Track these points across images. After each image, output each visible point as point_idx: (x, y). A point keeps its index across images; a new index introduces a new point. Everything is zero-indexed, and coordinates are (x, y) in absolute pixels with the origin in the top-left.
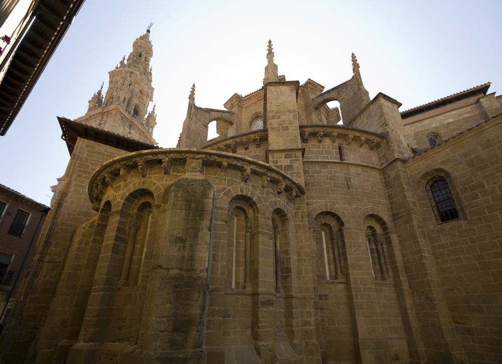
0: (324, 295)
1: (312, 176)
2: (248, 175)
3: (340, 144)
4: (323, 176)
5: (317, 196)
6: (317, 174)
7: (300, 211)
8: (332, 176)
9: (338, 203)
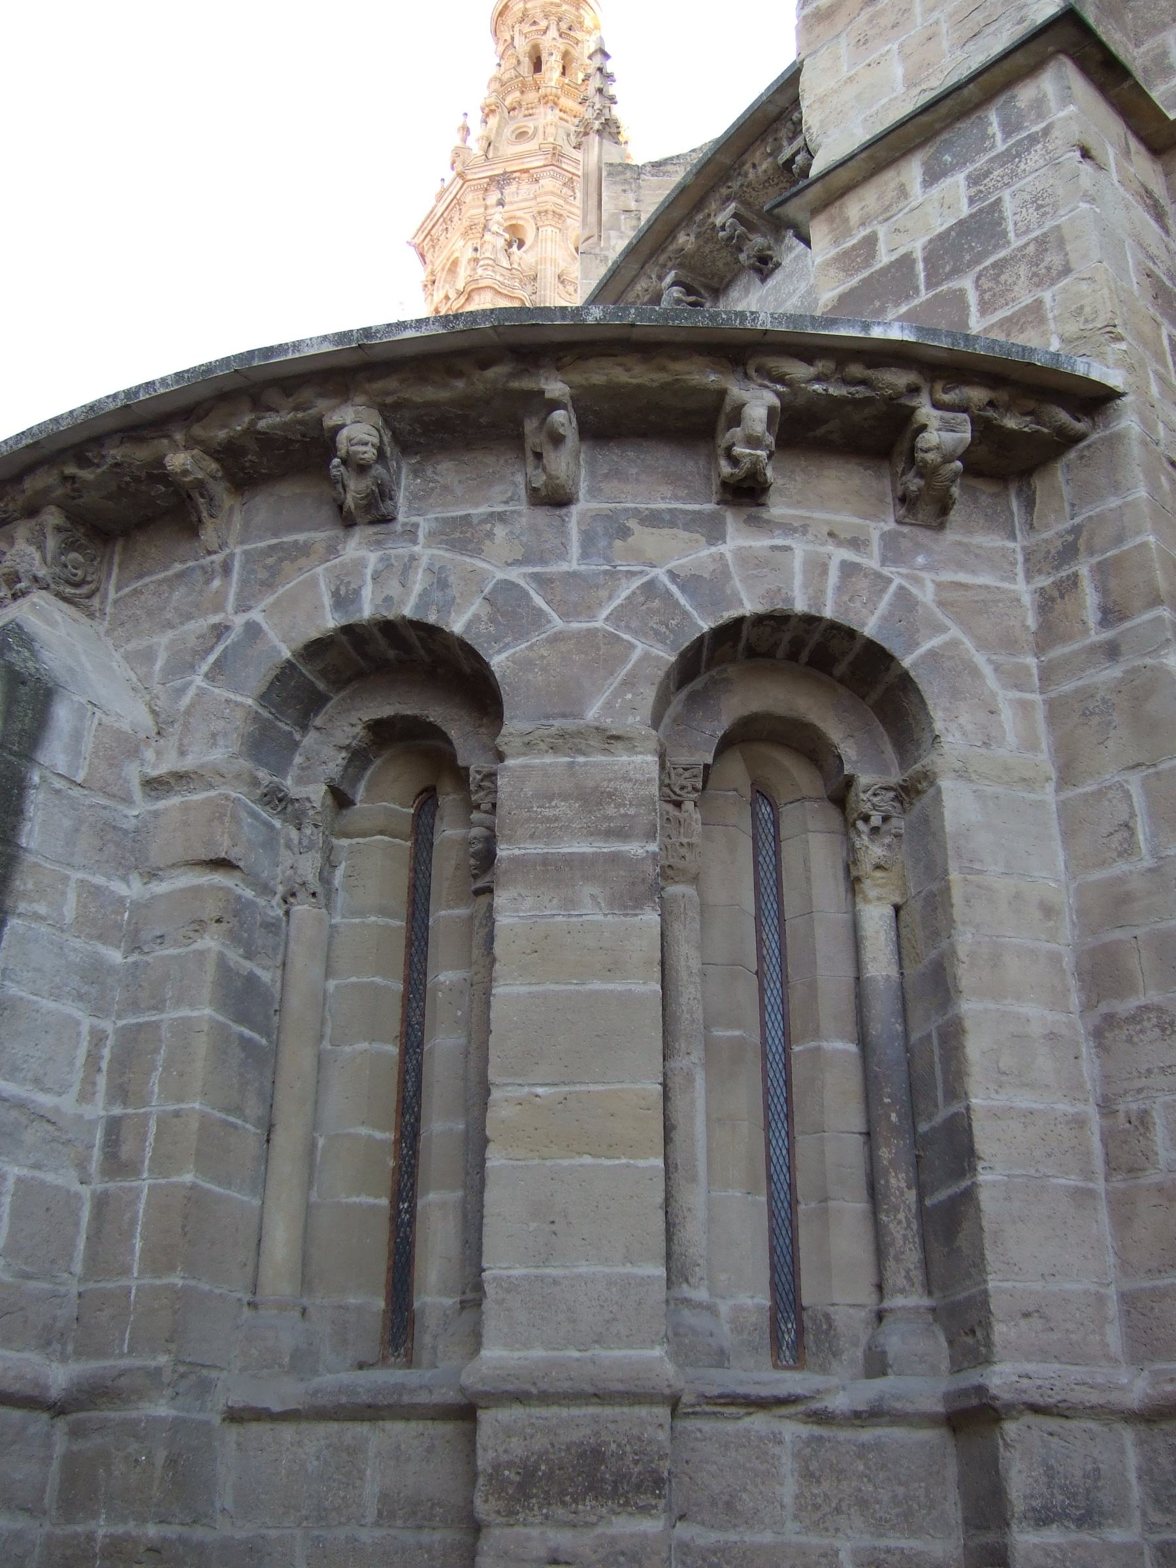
2: (362, 469)
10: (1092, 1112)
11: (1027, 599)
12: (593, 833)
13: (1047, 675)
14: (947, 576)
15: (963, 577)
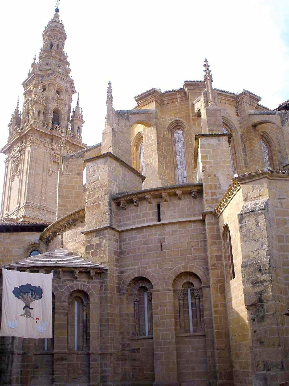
0: (136, 349)
1: (128, 244)
3: (158, 202)
6: (133, 241)
8: (146, 241)
10: (99, 332)
11: (99, 286)
12: (62, 310)
13: (100, 294)
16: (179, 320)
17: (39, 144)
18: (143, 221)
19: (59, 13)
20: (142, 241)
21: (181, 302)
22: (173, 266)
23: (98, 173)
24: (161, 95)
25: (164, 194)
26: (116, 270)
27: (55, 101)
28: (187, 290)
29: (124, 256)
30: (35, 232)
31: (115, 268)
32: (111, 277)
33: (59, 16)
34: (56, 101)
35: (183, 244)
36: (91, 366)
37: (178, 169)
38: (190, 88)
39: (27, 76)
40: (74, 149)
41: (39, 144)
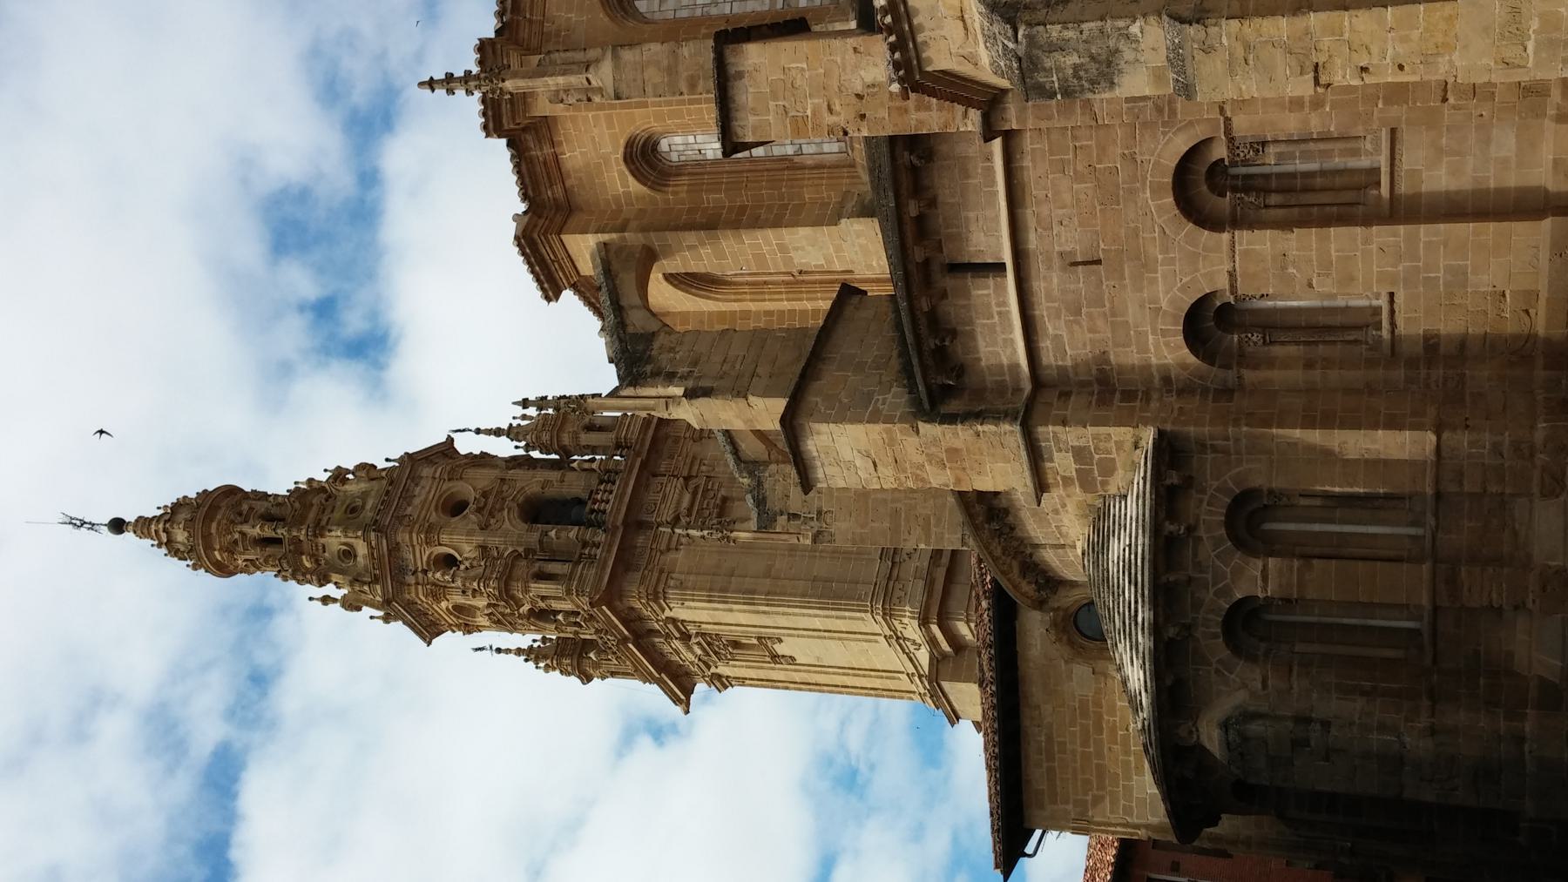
4: (1071, 332)
5: (1138, 353)
7: (1209, 443)
9: (1155, 300)
11: (1213, 455)
14: (1208, 477)
15: (1208, 472)
16: (1335, 209)
17: (661, 571)
18: (1005, 316)
19: (130, 517)
20: (1070, 321)
21: (1274, 199)
22: (1154, 227)
23: (847, 454)
24: (534, 213)
25: (918, 255)
26: (1160, 399)
27: (492, 521)
28: (1236, 177)
29: (1115, 375)
30: (1017, 622)
31: (1154, 405)
32: (1183, 418)
33: (140, 517)
34: (491, 515)
35: (1083, 197)
36: (1478, 490)
37: (799, 153)
38: (509, 114)
39: (398, 626)
40: (670, 441)
41: (661, 571)
